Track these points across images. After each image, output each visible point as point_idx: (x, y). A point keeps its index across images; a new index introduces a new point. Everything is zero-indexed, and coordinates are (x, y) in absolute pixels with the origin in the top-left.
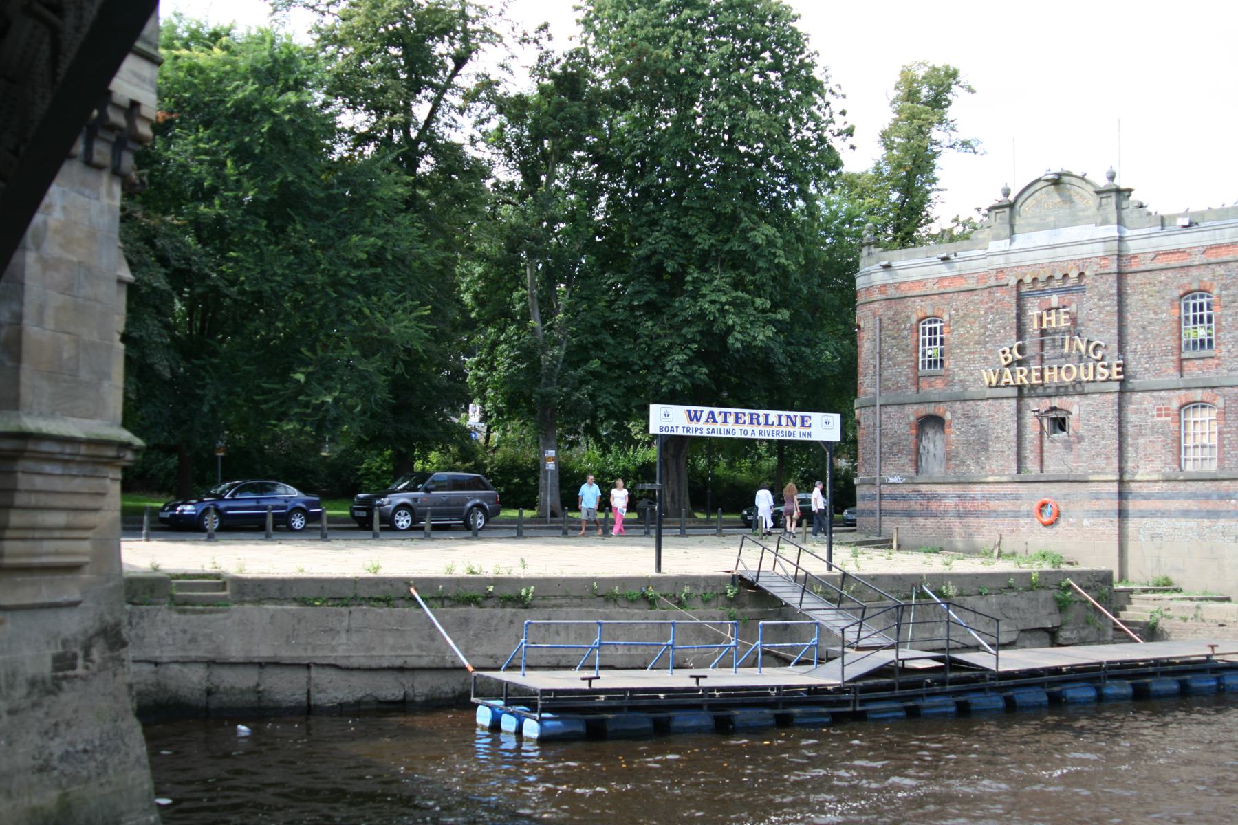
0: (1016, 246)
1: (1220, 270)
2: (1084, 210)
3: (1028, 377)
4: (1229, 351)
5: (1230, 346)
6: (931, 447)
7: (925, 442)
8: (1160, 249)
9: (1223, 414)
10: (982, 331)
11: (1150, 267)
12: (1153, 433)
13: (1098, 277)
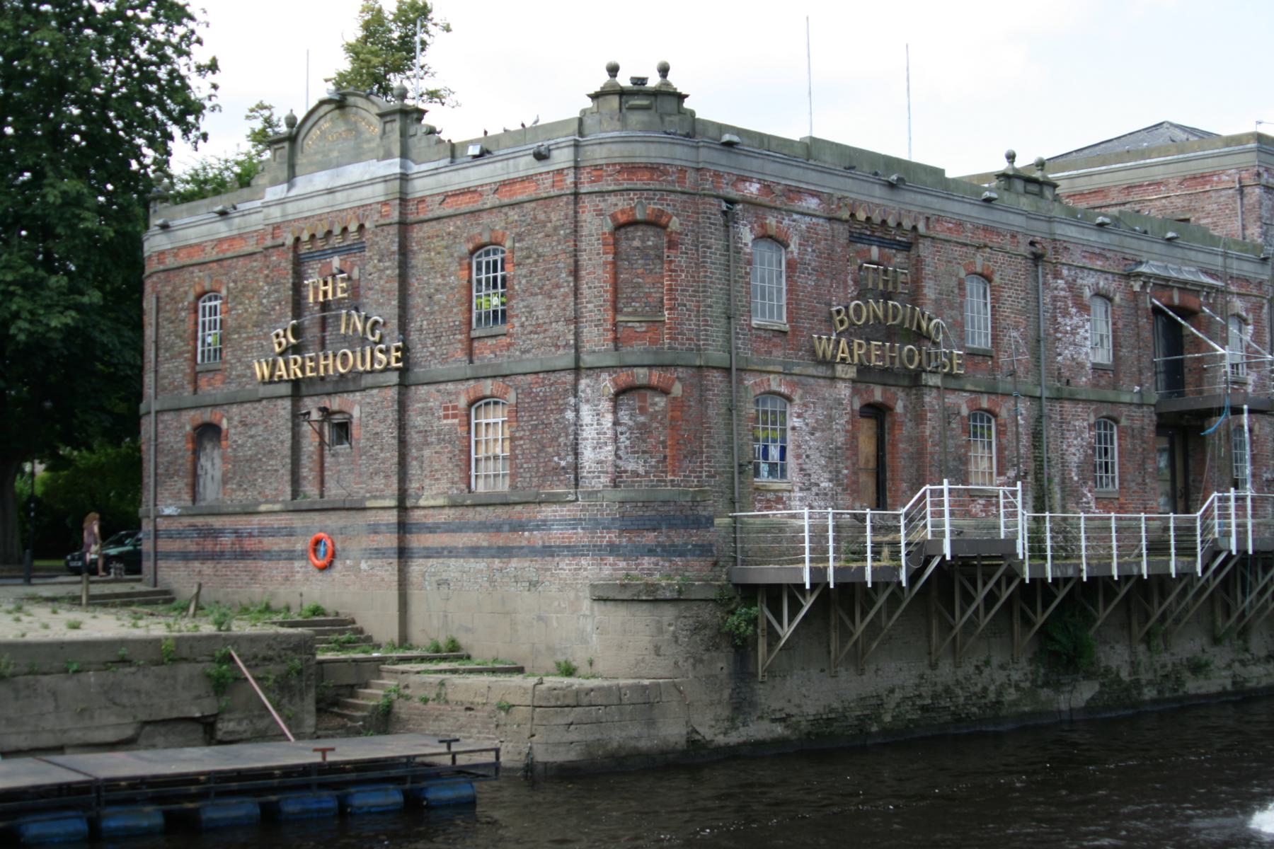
0: (294, 192)
1: (514, 215)
3: (303, 369)
4: (522, 326)
5: (524, 319)
6: (208, 465)
7: (203, 461)
8: (449, 189)
9: (515, 412)
11: (438, 213)
12: (439, 441)
13: (378, 230)
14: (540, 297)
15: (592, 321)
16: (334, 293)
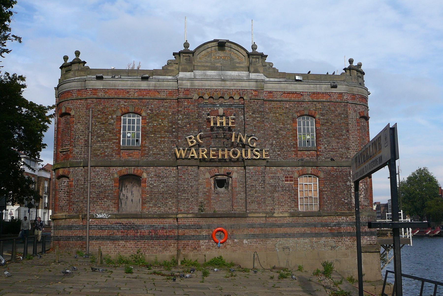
1: (319, 106)
2: (239, 63)
3: (208, 154)
5: (326, 146)
6: (129, 195)
8: (286, 90)
10: (170, 124)
11: (280, 99)
14: (333, 138)
15: (354, 150)
16: (228, 124)
